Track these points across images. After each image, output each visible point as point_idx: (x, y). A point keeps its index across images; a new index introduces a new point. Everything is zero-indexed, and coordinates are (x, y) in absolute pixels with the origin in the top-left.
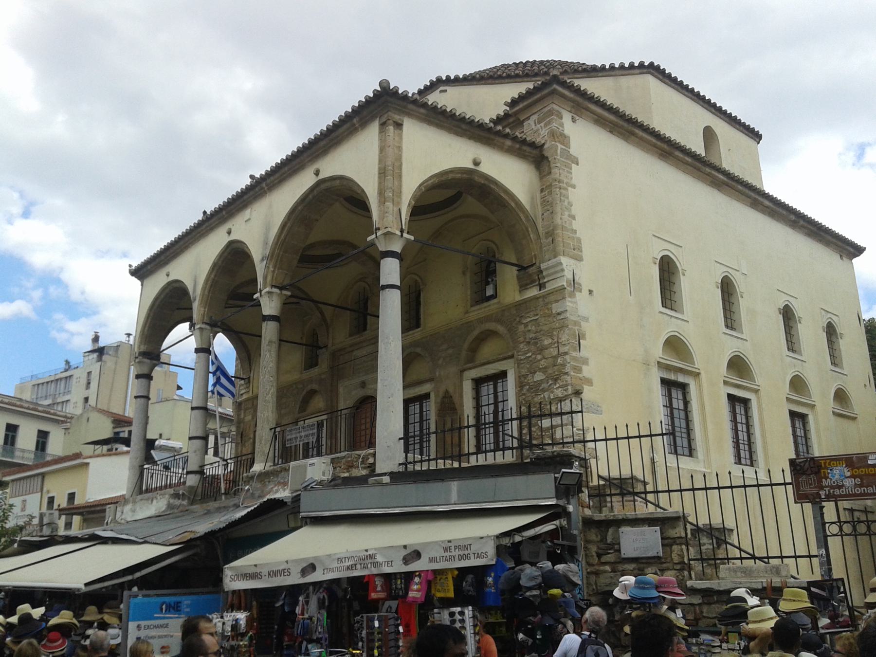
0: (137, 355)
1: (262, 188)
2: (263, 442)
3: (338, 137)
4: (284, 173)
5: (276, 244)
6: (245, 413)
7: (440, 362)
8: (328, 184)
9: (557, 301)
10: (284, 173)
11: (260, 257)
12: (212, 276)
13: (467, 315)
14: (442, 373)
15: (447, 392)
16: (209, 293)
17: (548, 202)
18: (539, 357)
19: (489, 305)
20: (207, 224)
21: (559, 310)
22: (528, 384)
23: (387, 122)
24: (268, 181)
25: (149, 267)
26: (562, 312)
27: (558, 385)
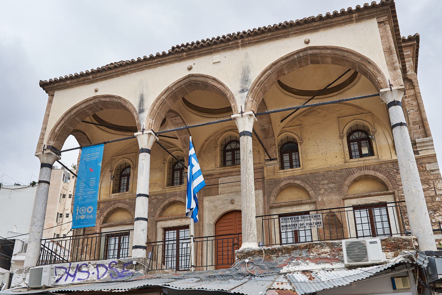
0: (45, 148)
1: (237, 43)
2: (253, 226)
3: (333, 22)
4: (265, 37)
5: (257, 83)
7: (322, 191)
8: (315, 51)
9: (429, 163)
10: (265, 37)
11: (240, 89)
12: (163, 97)
13: (347, 164)
14: (325, 199)
16: (158, 109)
17: (412, 104)
19: (369, 160)
20: (160, 59)
21: (433, 169)
23: (385, 22)
24: (246, 39)
26: (435, 170)
27: (438, 214)
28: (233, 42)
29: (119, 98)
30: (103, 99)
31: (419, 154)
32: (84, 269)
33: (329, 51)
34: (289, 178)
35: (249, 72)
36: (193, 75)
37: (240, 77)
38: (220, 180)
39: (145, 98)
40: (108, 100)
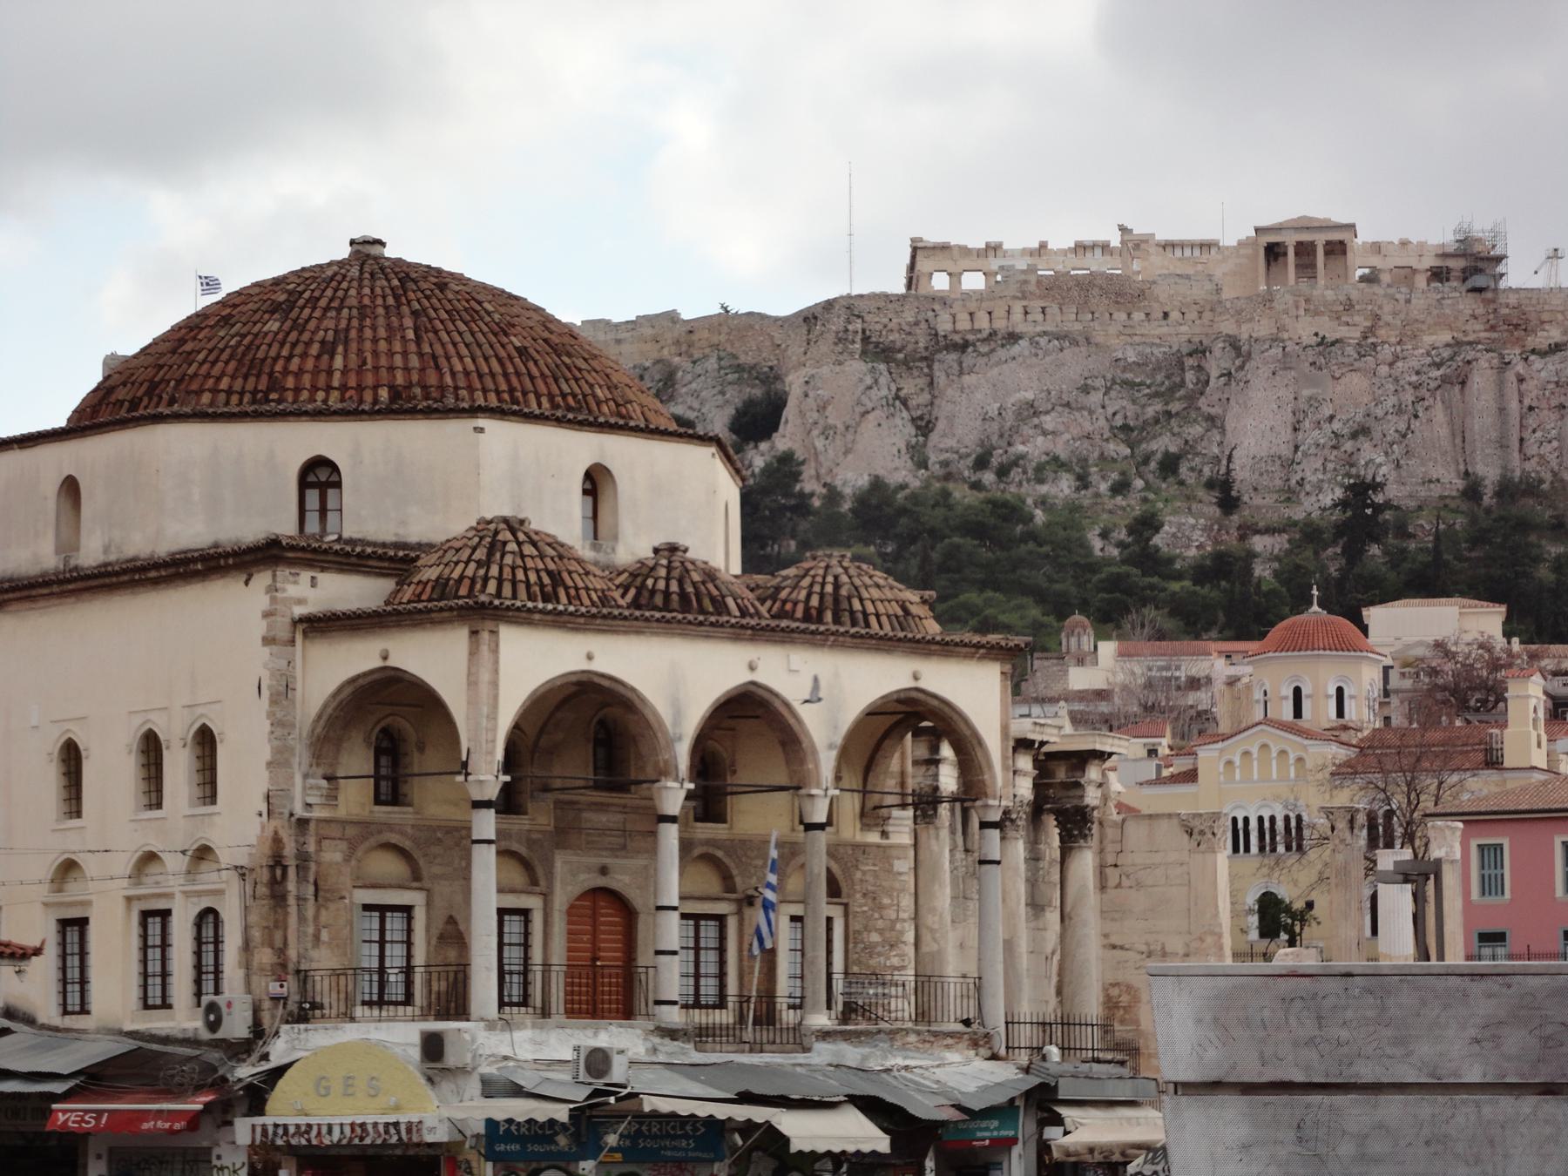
1: (827, 640)
6: (319, 842)
18: (876, 915)
22: (863, 942)
24: (841, 639)
25: (537, 616)
28: (823, 637)
29: (633, 690)
30: (597, 680)
31: (887, 838)
34: (708, 842)
36: (753, 683)
38: (585, 815)
40: (606, 683)
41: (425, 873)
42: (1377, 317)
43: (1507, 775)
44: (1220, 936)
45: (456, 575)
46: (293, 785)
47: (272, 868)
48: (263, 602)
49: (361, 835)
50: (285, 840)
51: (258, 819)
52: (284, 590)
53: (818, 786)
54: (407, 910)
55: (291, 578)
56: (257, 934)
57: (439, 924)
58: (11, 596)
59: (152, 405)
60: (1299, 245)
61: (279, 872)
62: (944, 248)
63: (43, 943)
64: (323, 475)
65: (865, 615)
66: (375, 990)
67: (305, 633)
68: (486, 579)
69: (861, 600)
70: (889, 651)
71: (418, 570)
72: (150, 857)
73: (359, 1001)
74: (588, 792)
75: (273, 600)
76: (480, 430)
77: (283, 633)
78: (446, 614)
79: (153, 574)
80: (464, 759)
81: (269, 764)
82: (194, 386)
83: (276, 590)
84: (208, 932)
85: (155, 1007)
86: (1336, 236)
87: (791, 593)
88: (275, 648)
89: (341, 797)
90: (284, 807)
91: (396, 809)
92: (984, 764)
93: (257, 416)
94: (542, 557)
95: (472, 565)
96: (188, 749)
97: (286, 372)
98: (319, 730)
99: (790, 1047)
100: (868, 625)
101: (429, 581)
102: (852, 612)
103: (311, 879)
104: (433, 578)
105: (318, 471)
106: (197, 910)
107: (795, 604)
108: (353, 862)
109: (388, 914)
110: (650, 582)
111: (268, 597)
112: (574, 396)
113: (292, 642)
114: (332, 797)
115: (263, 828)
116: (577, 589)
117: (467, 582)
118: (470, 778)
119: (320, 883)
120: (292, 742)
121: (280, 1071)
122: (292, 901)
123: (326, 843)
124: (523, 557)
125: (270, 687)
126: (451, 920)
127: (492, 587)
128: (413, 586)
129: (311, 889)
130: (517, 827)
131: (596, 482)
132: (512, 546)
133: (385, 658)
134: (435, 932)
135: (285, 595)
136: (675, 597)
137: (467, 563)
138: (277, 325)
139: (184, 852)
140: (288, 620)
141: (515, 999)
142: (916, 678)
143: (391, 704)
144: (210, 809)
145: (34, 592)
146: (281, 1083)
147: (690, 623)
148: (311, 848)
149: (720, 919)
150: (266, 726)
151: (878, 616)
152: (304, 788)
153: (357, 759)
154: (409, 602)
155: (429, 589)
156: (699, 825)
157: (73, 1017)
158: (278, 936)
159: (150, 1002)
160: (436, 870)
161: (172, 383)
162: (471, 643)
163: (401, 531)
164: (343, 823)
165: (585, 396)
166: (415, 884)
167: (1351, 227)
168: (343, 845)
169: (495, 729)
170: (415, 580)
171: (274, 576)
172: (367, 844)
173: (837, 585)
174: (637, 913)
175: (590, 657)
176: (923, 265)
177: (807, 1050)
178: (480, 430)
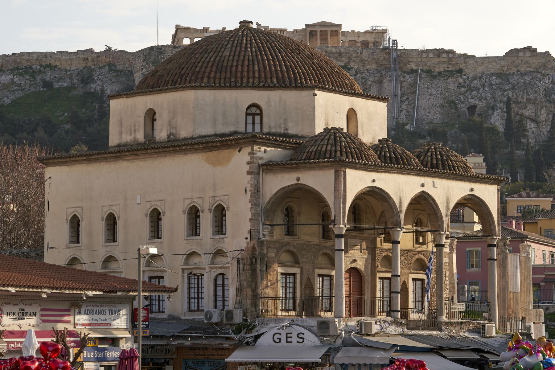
6: (267, 249)
15: (404, 281)
24: (450, 176)
25: (358, 166)
29: (387, 193)
30: (376, 190)
32: (378, 323)
33: (477, 200)
35: (449, 202)
37: (445, 204)
38: (349, 240)
39: (402, 200)
40: (378, 191)
41: (300, 261)
42: (350, 58)
43: (465, 225)
44: (454, 284)
45: (324, 149)
46: (259, 227)
47: (251, 259)
48: (248, 158)
49: (280, 247)
50: (257, 249)
51: (246, 240)
52: (256, 154)
53: (443, 231)
54: (294, 275)
55: (258, 149)
56: (245, 284)
57: (305, 280)
58: (127, 153)
59: (182, 82)
60: (321, 31)
61: (254, 260)
62: (188, 29)
63: (178, 286)
64: (254, 110)
65: (453, 167)
66: (291, 305)
67: (263, 172)
68: (336, 151)
69: (451, 161)
70: (464, 181)
71: (305, 147)
72: (193, 254)
73: (279, 310)
74: (351, 231)
75: (252, 158)
76: (316, 95)
77: (256, 171)
78: (326, 164)
79: (196, 147)
80: (333, 218)
81: (250, 220)
82: (200, 76)
83: (253, 154)
84: (219, 282)
85: (195, 311)
86: (334, 29)
87: (424, 158)
88: (253, 176)
89: (275, 232)
90: (256, 236)
91: (292, 237)
92: (492, 223)
93: (231, 87)
94: (354, 143)
95: (329, 146)
96: (212, 213)
97: (236, 71)
98: (268, 207)
99: (431, 328)
100: (455, 170)
101: (312, 152)
102: (449, 165)
103: (265, 264)
104: (315, 150)
105: (252, 108)
106: (216, 274)
107: (427, 162)
108: (278, 257)
109: (288, 276)
110: (383, 153)
111: (249, 157)
112: (339, 83)
113: (259, 174)
114: (271, 233)
115: (248, 243)
116: (368, 155)
117: (328, 153)
118: (336, 226)
119: (268, 265)
120: (259, 211)
121: (258, 337)
122: (258, 271)
123: (270, 249)
124: (348, 143)
125: (250, 191)
126: (309, 279)
127: (338, 154)
128: (306, 154)
129: (265, 267)
130: (329, 244)
131: (351, 115)
132: (343, 139)
133: (298, 179)
134: (304, 284)
135: (256, 156)
136: (394, 159)
137: (327, 145)
138: (228, 54)
139: (211, 254)
140: (257, 165)
141: (291, 308)
142: (472, 190)
143: (290, 197)
144: (223, 236)
145: (139, 152)
146: (259, 341)
147: (405, 169)
148: (265, 252)
149: (389, 279)
150: (249, 205)
151: (458, 167)
152: (263, 228)
153: (280, 219)
154: (305, 160)
155: (313, 154)
156: (385, 244)
157: (157, 314)
158: (253, 285)
159: (193, 309)
160: (304, 260)
161: (190, 74)
162: (335, 175)
163: (286, 132)
164: (275, 242)
165: (342, 82)
166: (297, 265)
167: (340, 26)
168: (275, 250)
169: (344, 208)
170: (307, 151)
171: (252, 149)
172: (282, 250)
173: (441, 155)
174: (364, 276)
175: (374, 181)
176: (180, 35)
177: (440, 329)
178: (316, 95)
